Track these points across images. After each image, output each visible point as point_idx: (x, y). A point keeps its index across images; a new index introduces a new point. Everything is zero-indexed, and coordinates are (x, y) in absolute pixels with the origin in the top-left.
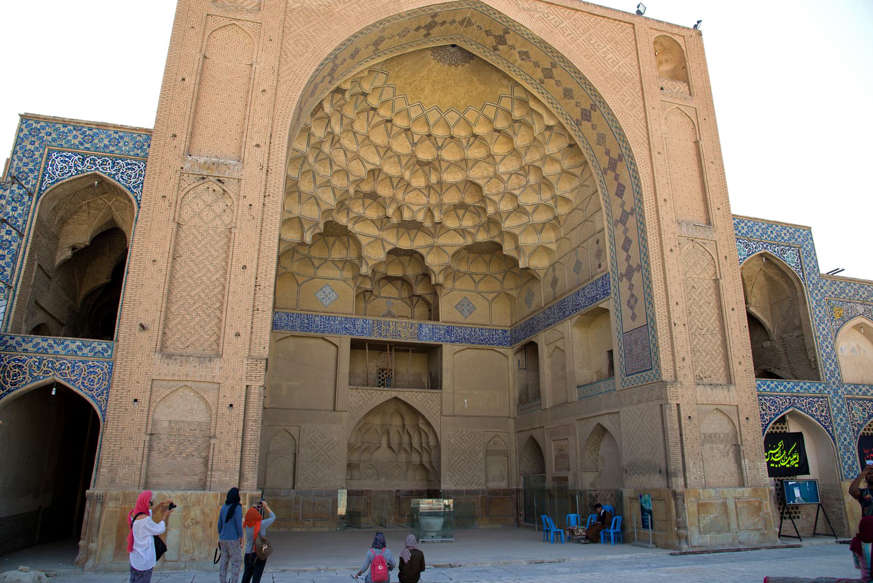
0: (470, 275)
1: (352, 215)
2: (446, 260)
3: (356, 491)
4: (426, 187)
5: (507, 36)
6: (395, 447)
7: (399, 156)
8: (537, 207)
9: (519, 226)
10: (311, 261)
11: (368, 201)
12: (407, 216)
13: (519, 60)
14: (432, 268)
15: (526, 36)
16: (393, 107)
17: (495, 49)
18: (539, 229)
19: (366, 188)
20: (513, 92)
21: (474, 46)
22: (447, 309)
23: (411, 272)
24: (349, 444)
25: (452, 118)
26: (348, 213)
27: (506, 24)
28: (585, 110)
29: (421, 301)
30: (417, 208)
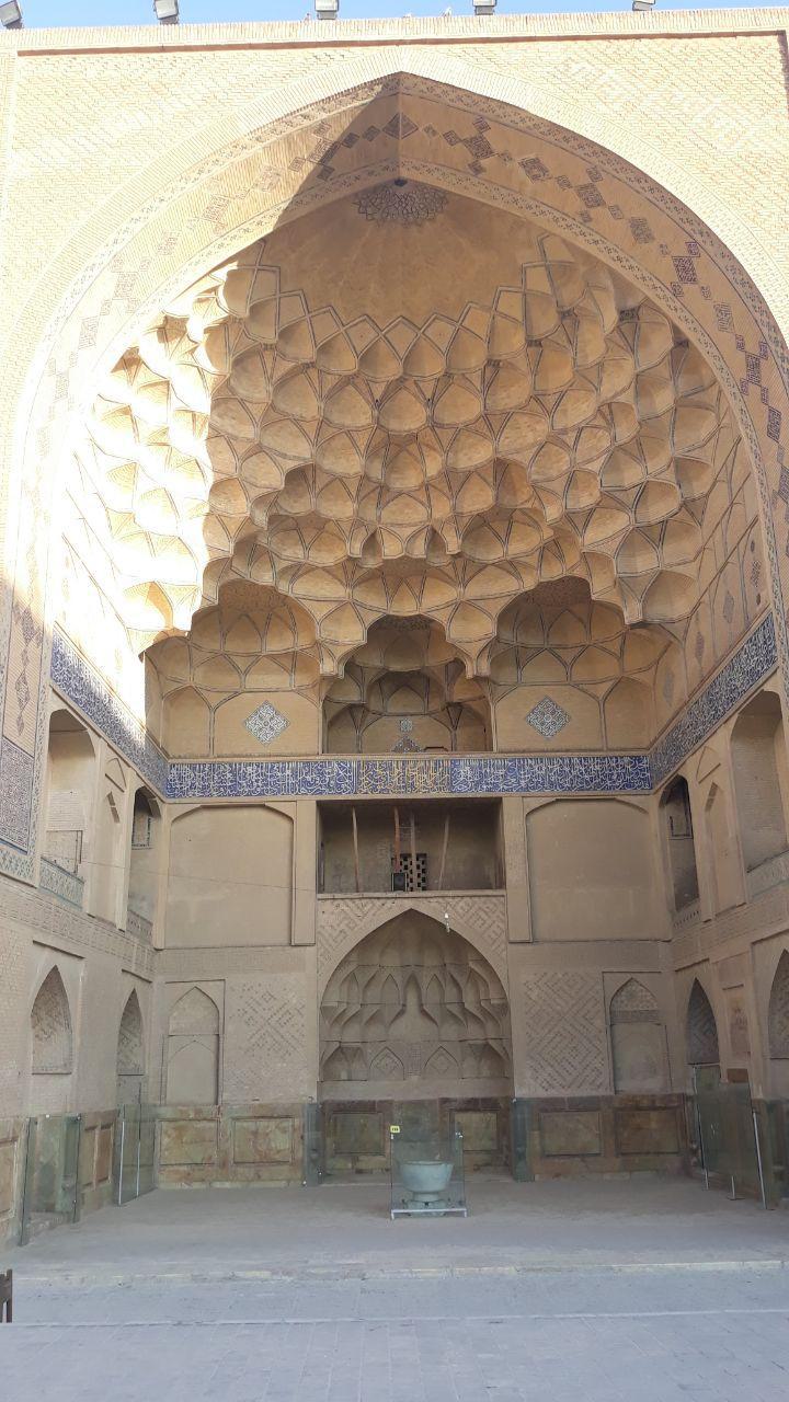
0: (551, 650)
3: (360, 1103)
6: (434, 1013)
9: (612, 538)
12: (391, 549)
13: (529, 181)
17: (478, 170)
18: (656, 537)
21: (436, 174)
23: (434, 661)
24: (324, 1011)
28: (681, 258)
30: (408, 531)
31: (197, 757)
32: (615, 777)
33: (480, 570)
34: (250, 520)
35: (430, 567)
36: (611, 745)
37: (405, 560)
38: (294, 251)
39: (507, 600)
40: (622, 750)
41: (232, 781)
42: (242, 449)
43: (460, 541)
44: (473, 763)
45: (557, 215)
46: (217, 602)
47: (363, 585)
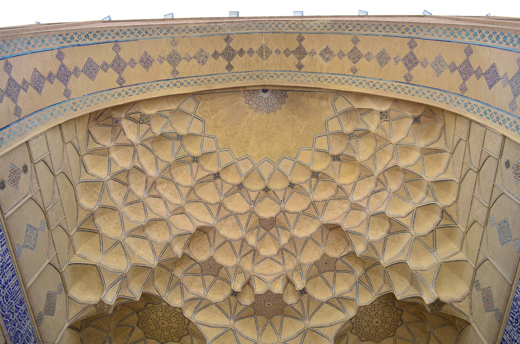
4: (278, 253)
5: (304, 43)
7: (236, 215)
8: (414, 214)
9: (403, 251)
11: (209, 279)
12: (260, 289)
13: (324, 63)
15: (319, 30)
17: (300, 67)
18: (430, 244)
19: (201, 256)
20: (335, 109)
25: (286, 166)
26: (182, 292)
27: (297, 30)
33: (319, 307)
34: (169, 245)
35: (285, 305)
37: (269, 292)
38: (213, 114)
39: (339, 326)
42: (172, 208)
43: (304, 282)
45: (340, 77)
46: (138, 299)
47: (242, 320)
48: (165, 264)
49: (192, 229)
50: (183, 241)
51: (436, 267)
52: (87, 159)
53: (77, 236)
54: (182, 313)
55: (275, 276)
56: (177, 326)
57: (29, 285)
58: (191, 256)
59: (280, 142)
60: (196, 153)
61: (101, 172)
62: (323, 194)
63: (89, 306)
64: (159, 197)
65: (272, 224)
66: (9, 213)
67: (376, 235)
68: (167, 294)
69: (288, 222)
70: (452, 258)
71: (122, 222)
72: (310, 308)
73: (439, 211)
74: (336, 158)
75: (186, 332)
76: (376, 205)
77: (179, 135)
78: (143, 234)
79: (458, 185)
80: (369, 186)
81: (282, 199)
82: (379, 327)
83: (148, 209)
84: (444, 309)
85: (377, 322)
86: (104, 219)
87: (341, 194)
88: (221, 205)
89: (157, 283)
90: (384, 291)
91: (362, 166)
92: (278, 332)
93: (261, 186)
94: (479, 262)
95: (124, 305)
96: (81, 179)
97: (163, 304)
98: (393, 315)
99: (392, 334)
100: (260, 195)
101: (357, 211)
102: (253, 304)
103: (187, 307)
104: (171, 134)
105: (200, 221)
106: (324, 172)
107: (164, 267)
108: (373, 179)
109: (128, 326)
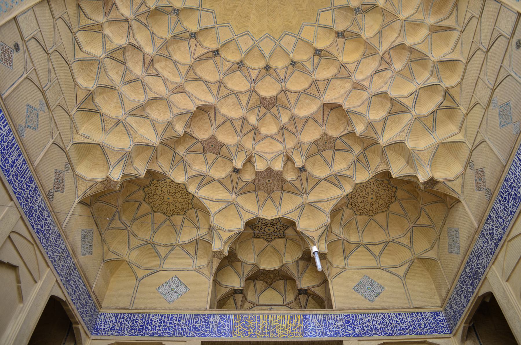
1: (191, 173)
2: (325, 219)
4: (279, 132)
7: (237, 94)
8: (416, 95)
9: (402, 131)
10: (155, 249)
11: (211, 157)
12: (260, 166)
14: (307, 233)
16: (218, 38)
18: (430, 124)
19: (203, 135)
22: (343, 293)
23: (289, 258)
25: (288, 43)
26: (185, 169)
29: (311, 301)
31: (120, 309)
32: (423, 326)
33: (317, 184)
34: (170, 124)
35: (285, 181)
36: (415, 304)
39: (335, 202)
40: (425, 308)
41: (141, 326)
42: (171, 87)
43: (304, 160)
44: (319, 317)
46: (143, 176)
48: (168, 142)
49: (192, 108)
50: (184, 120)
51: (433, 148)
52: (80, 36)
53: (78, 117)
54: (186, 189)
55: (275, 154)
56: (182, 200)
57: (36, 164)
58: (193, 135)
59: (282, 17)
60: (194, 28)
61: (96, 50)
62: (325, 73)
63: (96, 183)
64: (158, 75)
65: (273, 103)
66: (7, 94)
67: (376, 115)
68: (171, 171)
69: (289, 102)
70: (450, 139)
71: (122, 101)
72: (308, 184)
73: (442, 92)
74: (340, 35)
75: (191, 207)
76: (379, 85)
77: (175, 9)
78: (143, 114)
79: (464, 66)
80: (373, 65)
81: (283, 78)
82: (373, 203)
83: (147, 88)
84: (437, 187)
85: (372, 198)
86: (104, 99)
87: (343, 72)
88: (221, 83)
89: (160, 161)
90: (381, 169)
91: (367, 44)
92: (278, 206)
93: (262, 64)
94: (476, 143)
95: (130, 182)
96: (76, 57)
97: (167, 180)
98: (387, 192)
99: (386, 209)
100: (261, 73)
101: (359, 91)
102: (254, 180)
103: (191, 184)
104: (167, 8)
105: (201, 100)
106: (327, 50)
107: (166, 145)
108: (378, 58)
109: (136, 201)
